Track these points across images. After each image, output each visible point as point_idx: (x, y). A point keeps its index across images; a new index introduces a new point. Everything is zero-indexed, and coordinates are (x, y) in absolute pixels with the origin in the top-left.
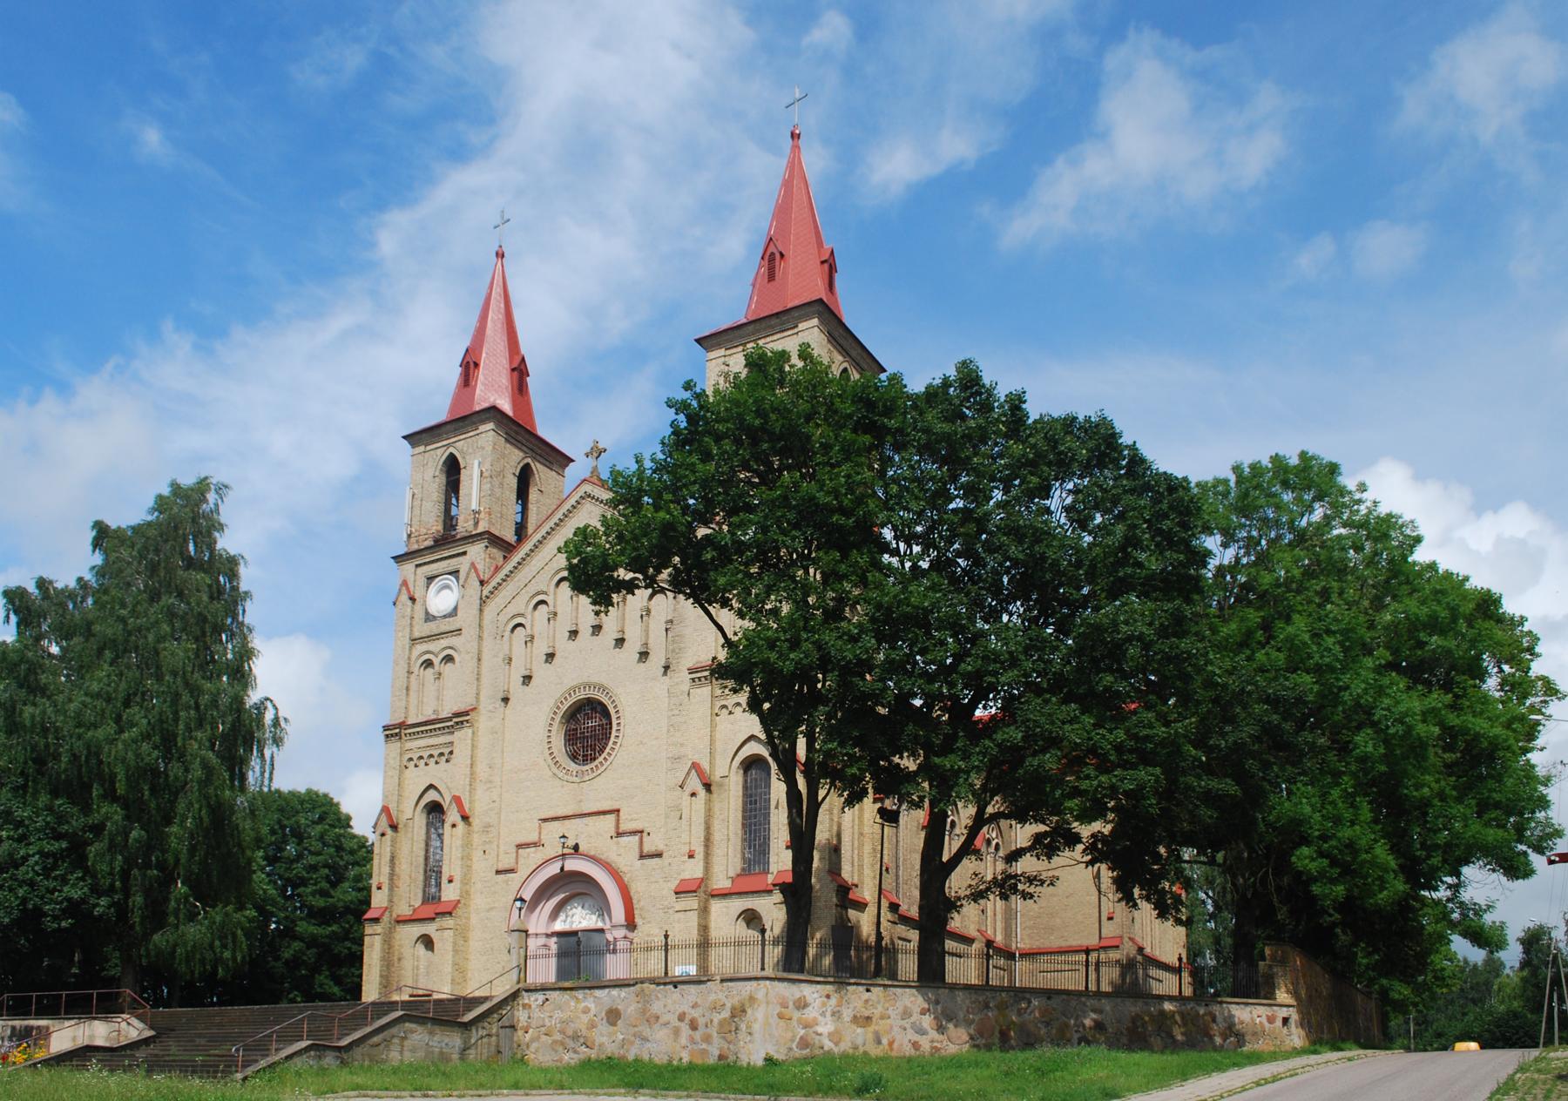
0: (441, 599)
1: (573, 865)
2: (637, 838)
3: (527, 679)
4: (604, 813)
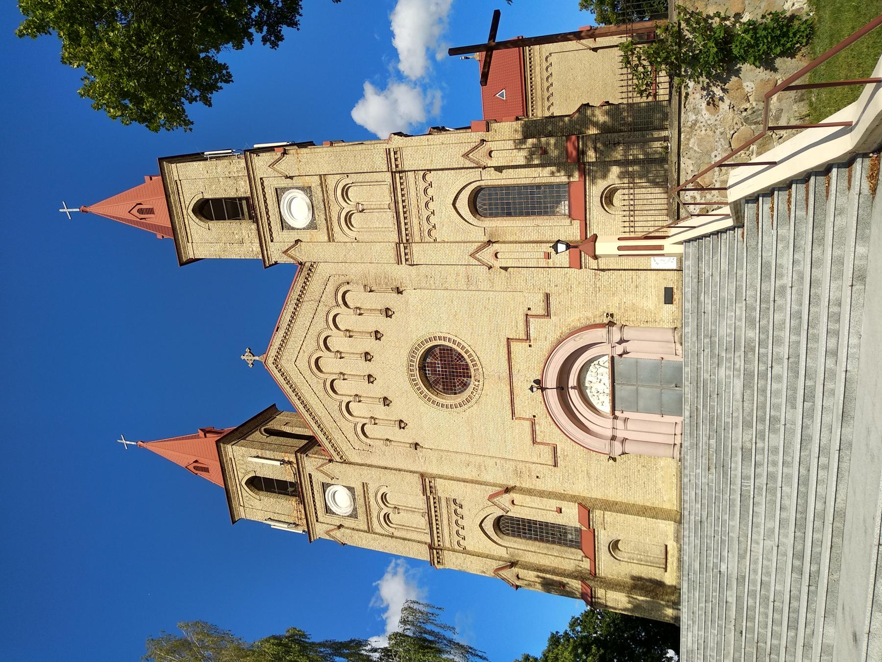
1: (551, 381)
2: (531, 320)
3: (402, 425)
4: (509, 353)
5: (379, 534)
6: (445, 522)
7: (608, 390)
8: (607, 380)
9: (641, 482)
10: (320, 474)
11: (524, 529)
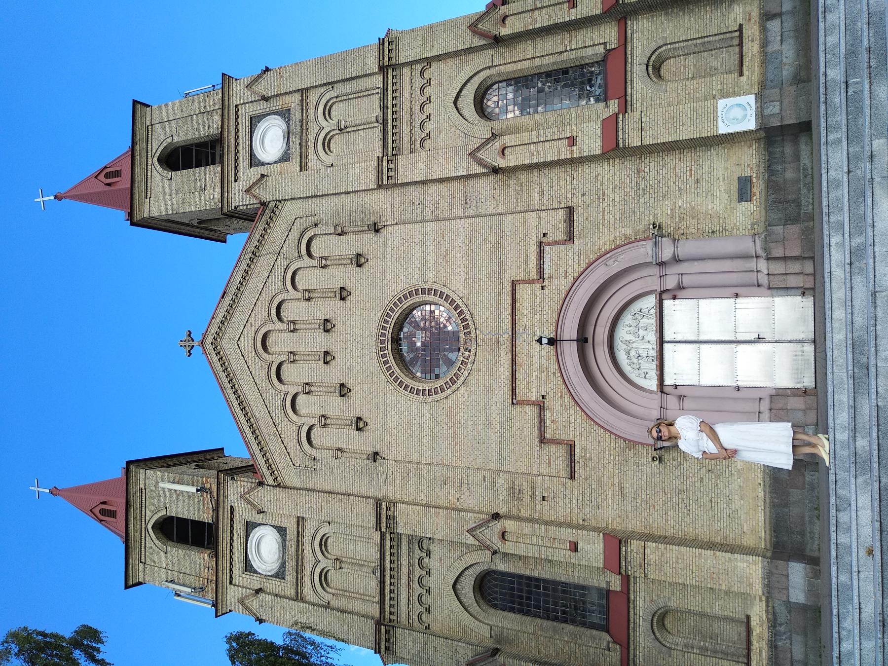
0: (266, 549)
1: (570, 330)
3: (360, 424)
5: (310, 603)
6: (404, 580)
7: (653, 353)
8: (652, 337)
9: (706, 499)
10: (245, 505)
11: (521, 597)
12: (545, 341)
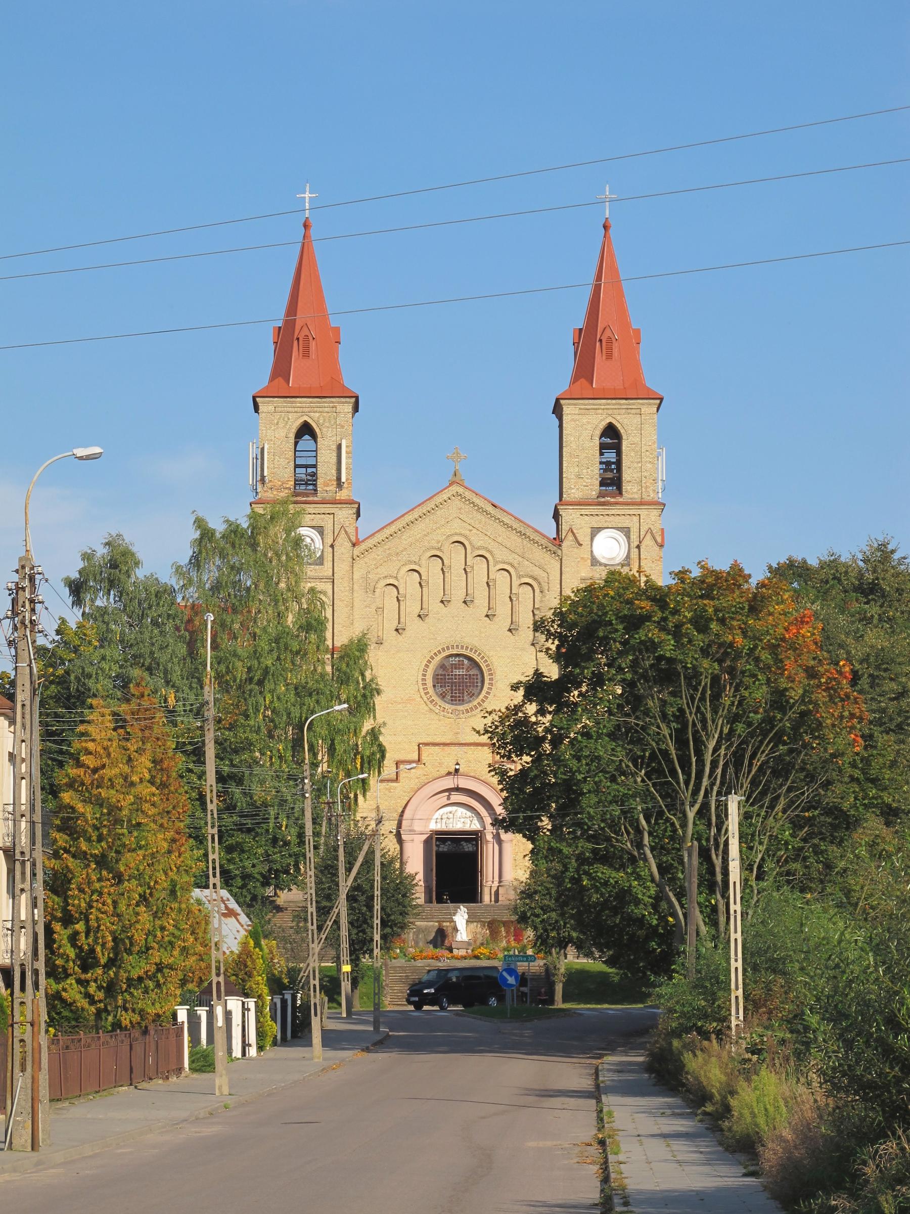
1: (463, 783)
12: (457, 767)
